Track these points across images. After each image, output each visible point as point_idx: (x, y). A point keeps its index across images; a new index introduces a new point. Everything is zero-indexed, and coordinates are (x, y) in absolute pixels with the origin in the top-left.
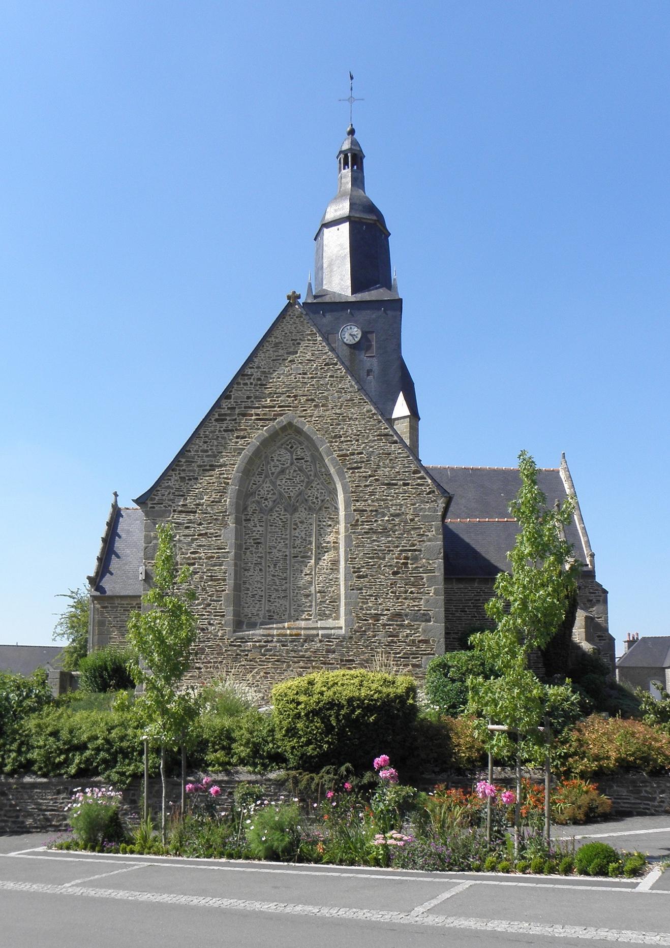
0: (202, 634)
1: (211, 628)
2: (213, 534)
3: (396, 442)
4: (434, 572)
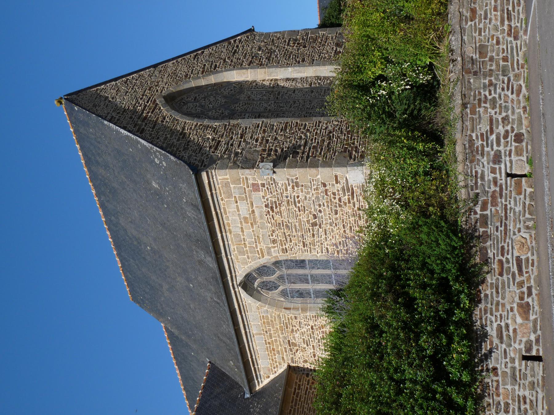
0: (334, 133)
1: (330, 128)
2: (243, 132)
3: (203, 52)
4: (308, 33)
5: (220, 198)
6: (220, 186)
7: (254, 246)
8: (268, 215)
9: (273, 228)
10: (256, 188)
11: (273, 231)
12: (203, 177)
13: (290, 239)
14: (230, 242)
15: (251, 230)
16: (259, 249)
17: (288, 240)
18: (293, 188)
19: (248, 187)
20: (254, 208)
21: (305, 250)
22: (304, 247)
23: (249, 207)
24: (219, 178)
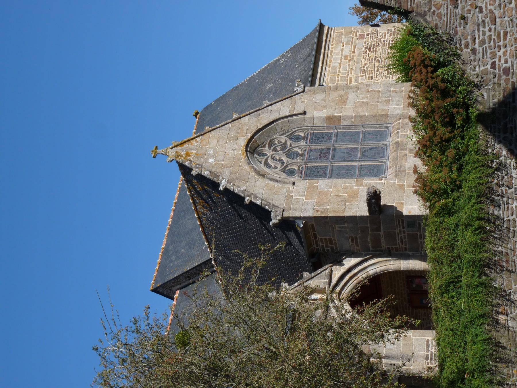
5: (331, 44)
6: (334, 37)
7: (346, 76)
8: (365, 54)
9: (366, 62)
10: (362, 36)
11: (365, 64)
12: (325, 29)
13: (378, 69)
14: (326, 73)
15: (347, 65)
16: (349, 78)
17: (376, 70)
18: (390, 35)
19: (356, 36)
20: (356, 50)
21: (388, 77)
22: (388, 74)
23: (351, 49)
24: (336, 31)
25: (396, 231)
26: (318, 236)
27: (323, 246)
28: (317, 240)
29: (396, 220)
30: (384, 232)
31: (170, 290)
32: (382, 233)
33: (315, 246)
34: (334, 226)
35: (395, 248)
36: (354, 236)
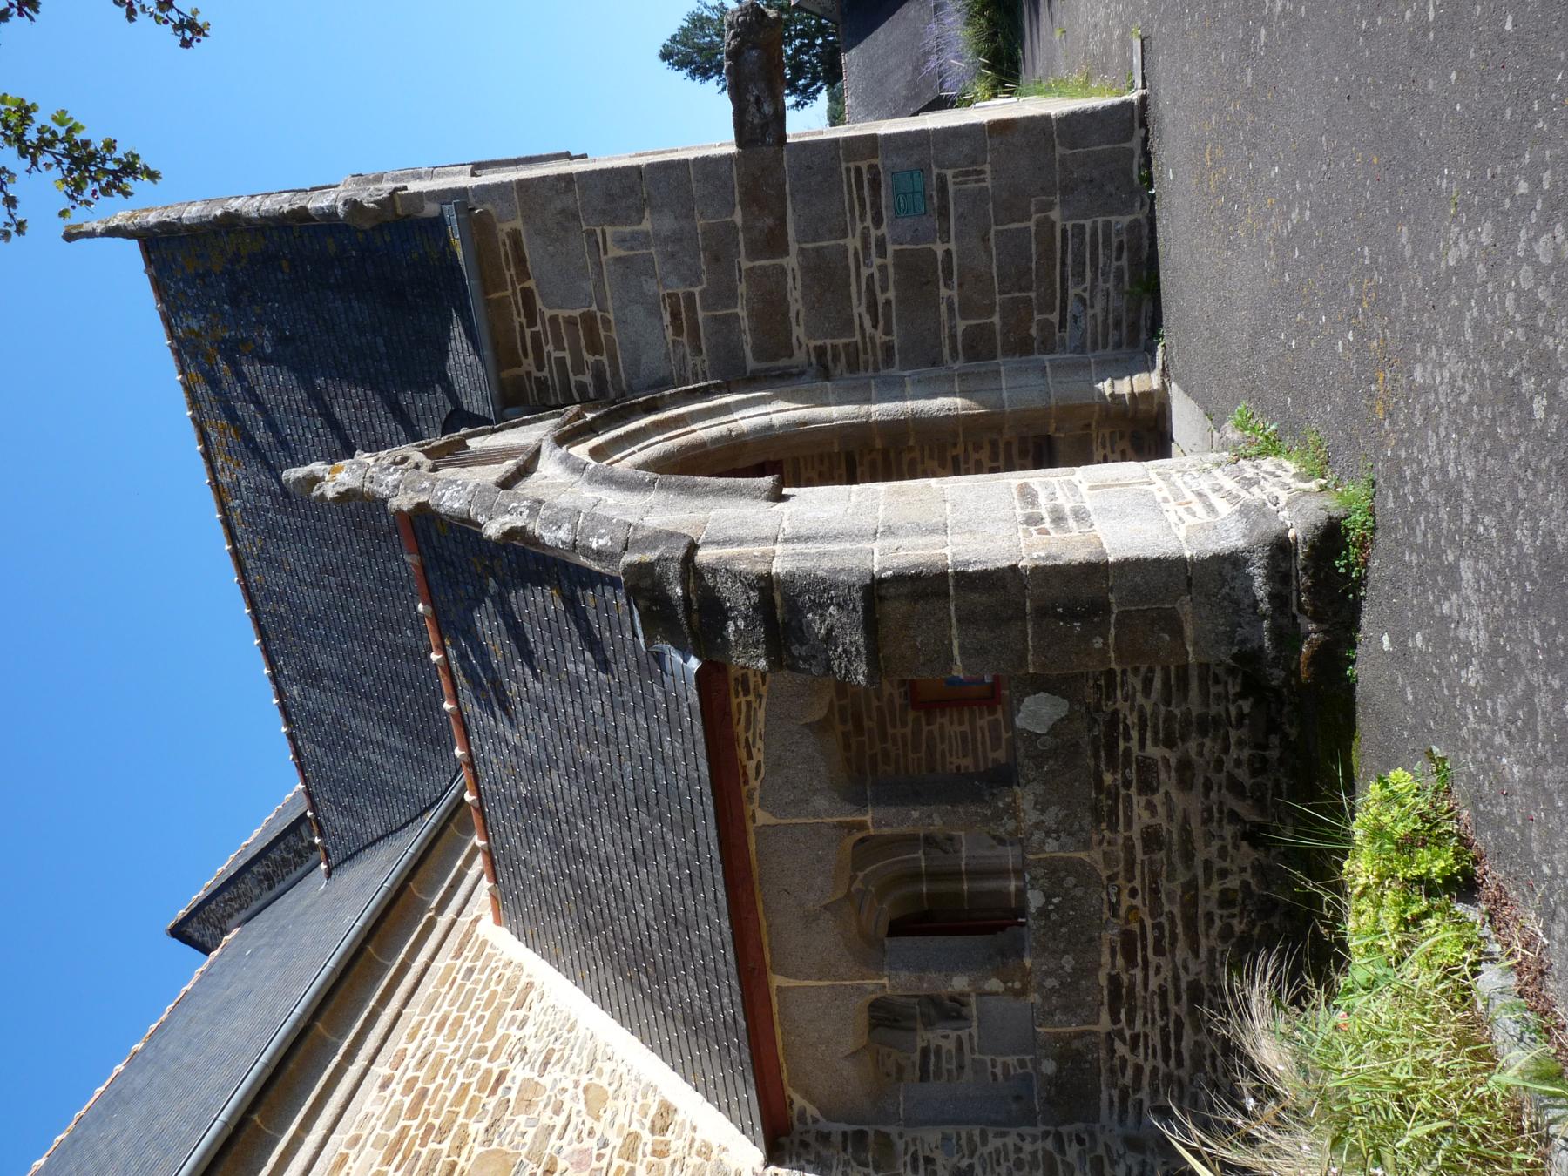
25: (853, 243)
26: (539, 304)
27: (560, 362)
28: (538, 328)
29: (848, 170)
30: (802, 251)
31: (221, 929)
32: (791, 262)
33: (529, 363)
34: (598, 231)
35: (846, 346)
36: (681, 291)
